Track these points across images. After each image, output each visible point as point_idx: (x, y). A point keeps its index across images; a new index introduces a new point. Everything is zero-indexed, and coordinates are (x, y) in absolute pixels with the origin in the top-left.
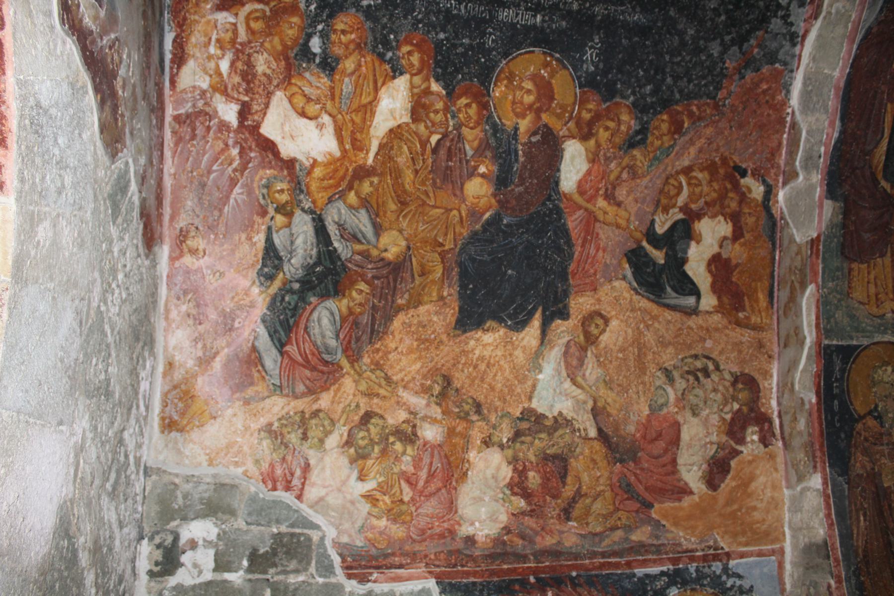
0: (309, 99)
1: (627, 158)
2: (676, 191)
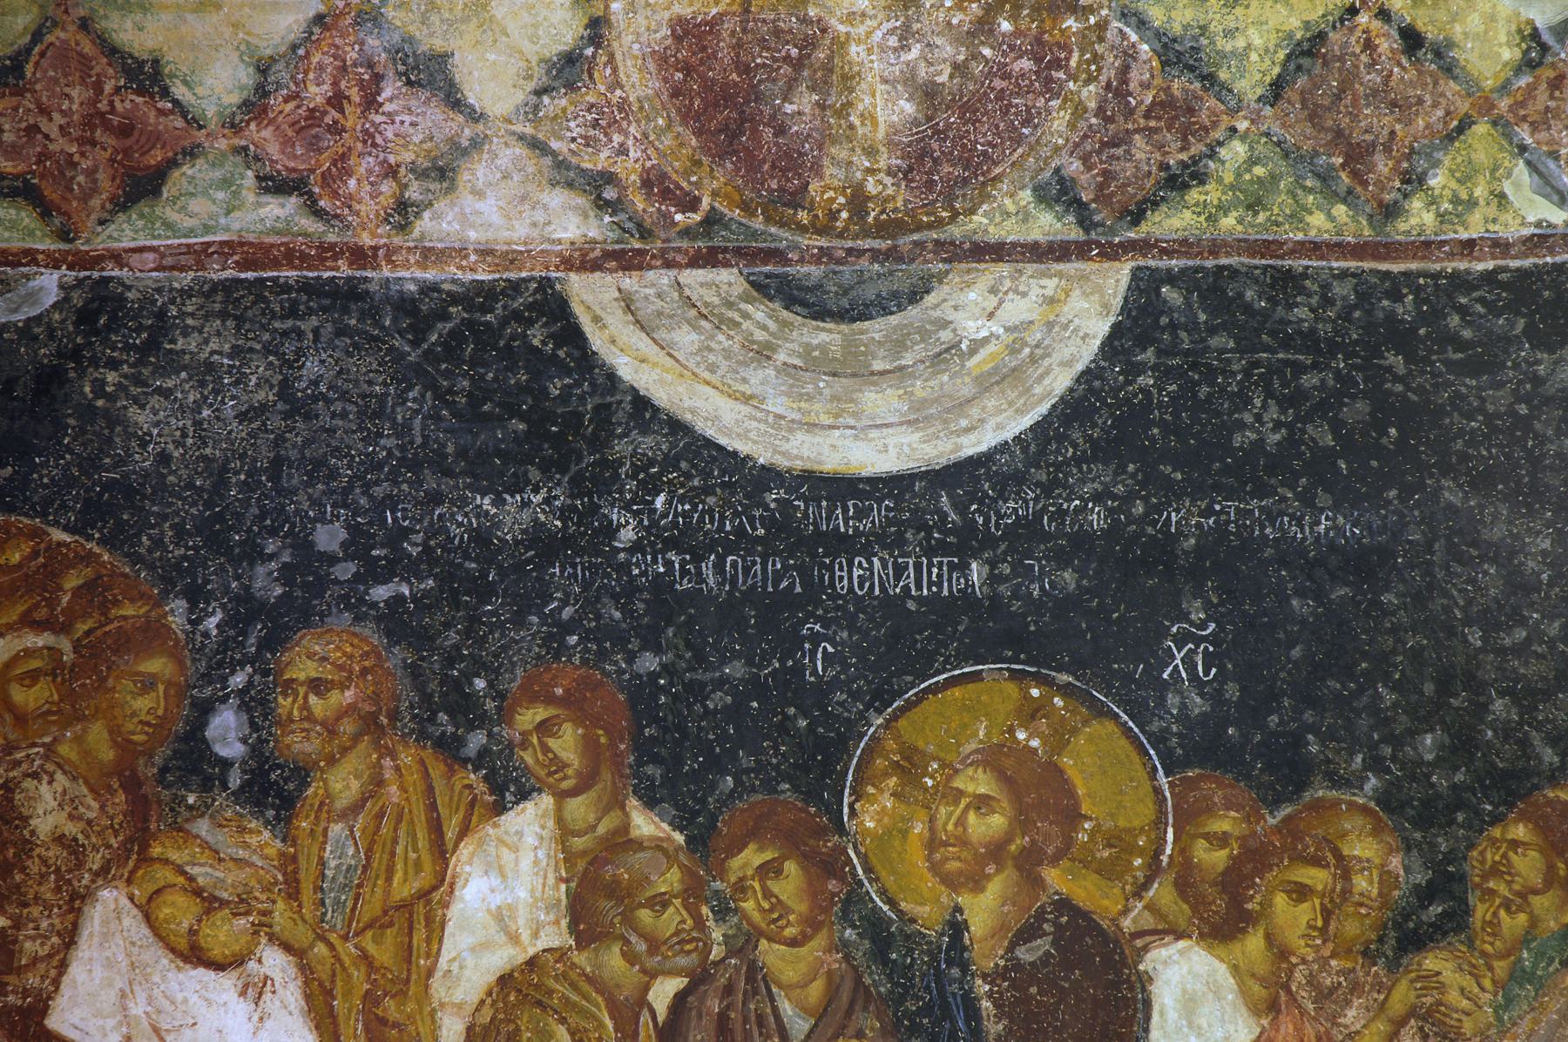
0: (210, 903)
1: (1403, 985)
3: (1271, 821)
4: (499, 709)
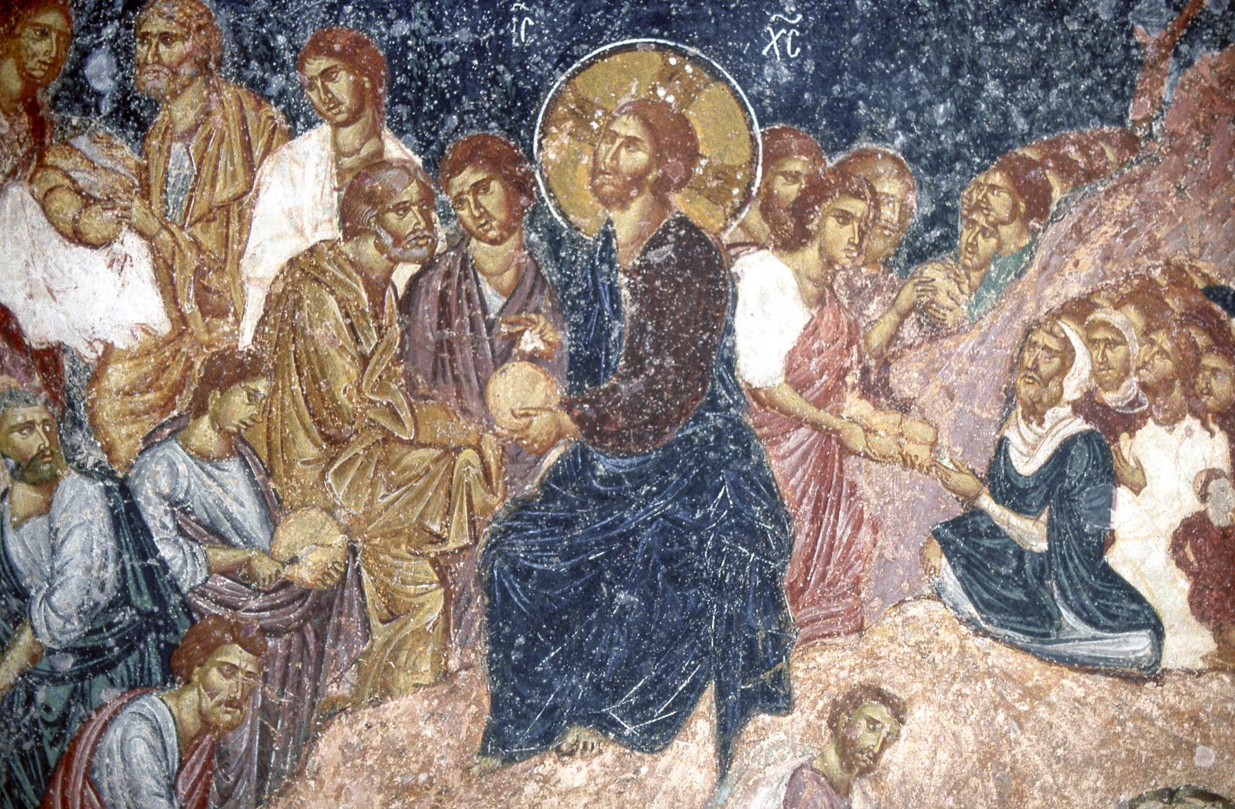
0: (88, 200)
2: (1057, 361)
3: (830, 165)
4: (295, 59)
